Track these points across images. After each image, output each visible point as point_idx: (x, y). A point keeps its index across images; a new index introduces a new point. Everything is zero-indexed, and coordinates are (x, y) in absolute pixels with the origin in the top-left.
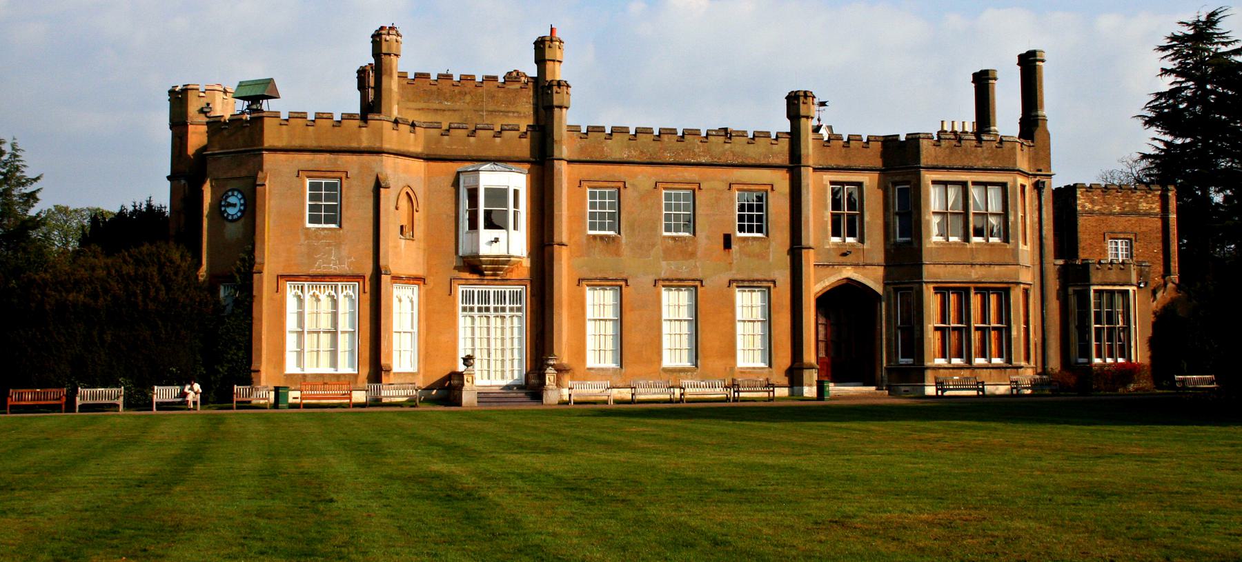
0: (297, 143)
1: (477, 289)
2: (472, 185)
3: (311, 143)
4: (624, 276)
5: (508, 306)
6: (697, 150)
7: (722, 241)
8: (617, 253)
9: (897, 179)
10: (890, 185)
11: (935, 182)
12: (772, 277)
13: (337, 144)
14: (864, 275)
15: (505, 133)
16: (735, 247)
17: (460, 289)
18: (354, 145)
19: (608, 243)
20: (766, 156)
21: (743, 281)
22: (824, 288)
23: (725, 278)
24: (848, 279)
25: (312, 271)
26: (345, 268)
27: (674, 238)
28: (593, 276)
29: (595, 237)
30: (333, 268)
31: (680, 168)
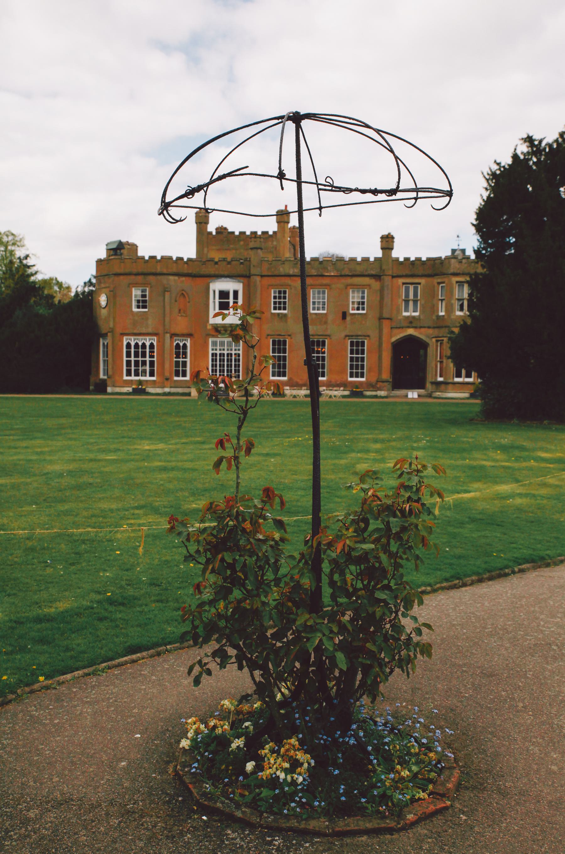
0: (127, 271)
1: (218, 340)
2: (214, 288)
3: (135, 271)
4: (289, 333)
5: (218, 348)
6: (329, 268)
7: (341, 315)
8: (286, 321)
9: (439, 280)
10: (436, 284)
11: (457, 282)
12: (368, 334)
13: (145, 271)
14: (421, 333)
15: (233, 263)
16: (348, 318)
17: (210, 340)
18: (153, 271)
19: (282, 318)
20: (366, 270)
21: (352, 336)
22: (397, 340)
23: (343, 335)
24: (410, 335)
25: (135, 331)
26: (150, 330)
27: (316, 314)
28: (273, 333)
29: (274, 314)
30: (144, 330)
31: (320, 278)
